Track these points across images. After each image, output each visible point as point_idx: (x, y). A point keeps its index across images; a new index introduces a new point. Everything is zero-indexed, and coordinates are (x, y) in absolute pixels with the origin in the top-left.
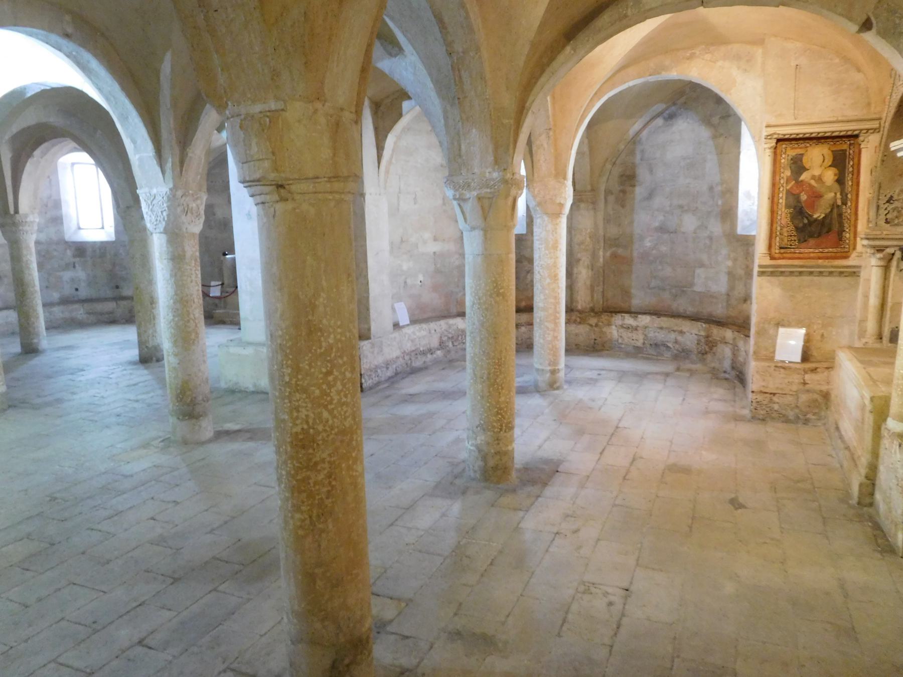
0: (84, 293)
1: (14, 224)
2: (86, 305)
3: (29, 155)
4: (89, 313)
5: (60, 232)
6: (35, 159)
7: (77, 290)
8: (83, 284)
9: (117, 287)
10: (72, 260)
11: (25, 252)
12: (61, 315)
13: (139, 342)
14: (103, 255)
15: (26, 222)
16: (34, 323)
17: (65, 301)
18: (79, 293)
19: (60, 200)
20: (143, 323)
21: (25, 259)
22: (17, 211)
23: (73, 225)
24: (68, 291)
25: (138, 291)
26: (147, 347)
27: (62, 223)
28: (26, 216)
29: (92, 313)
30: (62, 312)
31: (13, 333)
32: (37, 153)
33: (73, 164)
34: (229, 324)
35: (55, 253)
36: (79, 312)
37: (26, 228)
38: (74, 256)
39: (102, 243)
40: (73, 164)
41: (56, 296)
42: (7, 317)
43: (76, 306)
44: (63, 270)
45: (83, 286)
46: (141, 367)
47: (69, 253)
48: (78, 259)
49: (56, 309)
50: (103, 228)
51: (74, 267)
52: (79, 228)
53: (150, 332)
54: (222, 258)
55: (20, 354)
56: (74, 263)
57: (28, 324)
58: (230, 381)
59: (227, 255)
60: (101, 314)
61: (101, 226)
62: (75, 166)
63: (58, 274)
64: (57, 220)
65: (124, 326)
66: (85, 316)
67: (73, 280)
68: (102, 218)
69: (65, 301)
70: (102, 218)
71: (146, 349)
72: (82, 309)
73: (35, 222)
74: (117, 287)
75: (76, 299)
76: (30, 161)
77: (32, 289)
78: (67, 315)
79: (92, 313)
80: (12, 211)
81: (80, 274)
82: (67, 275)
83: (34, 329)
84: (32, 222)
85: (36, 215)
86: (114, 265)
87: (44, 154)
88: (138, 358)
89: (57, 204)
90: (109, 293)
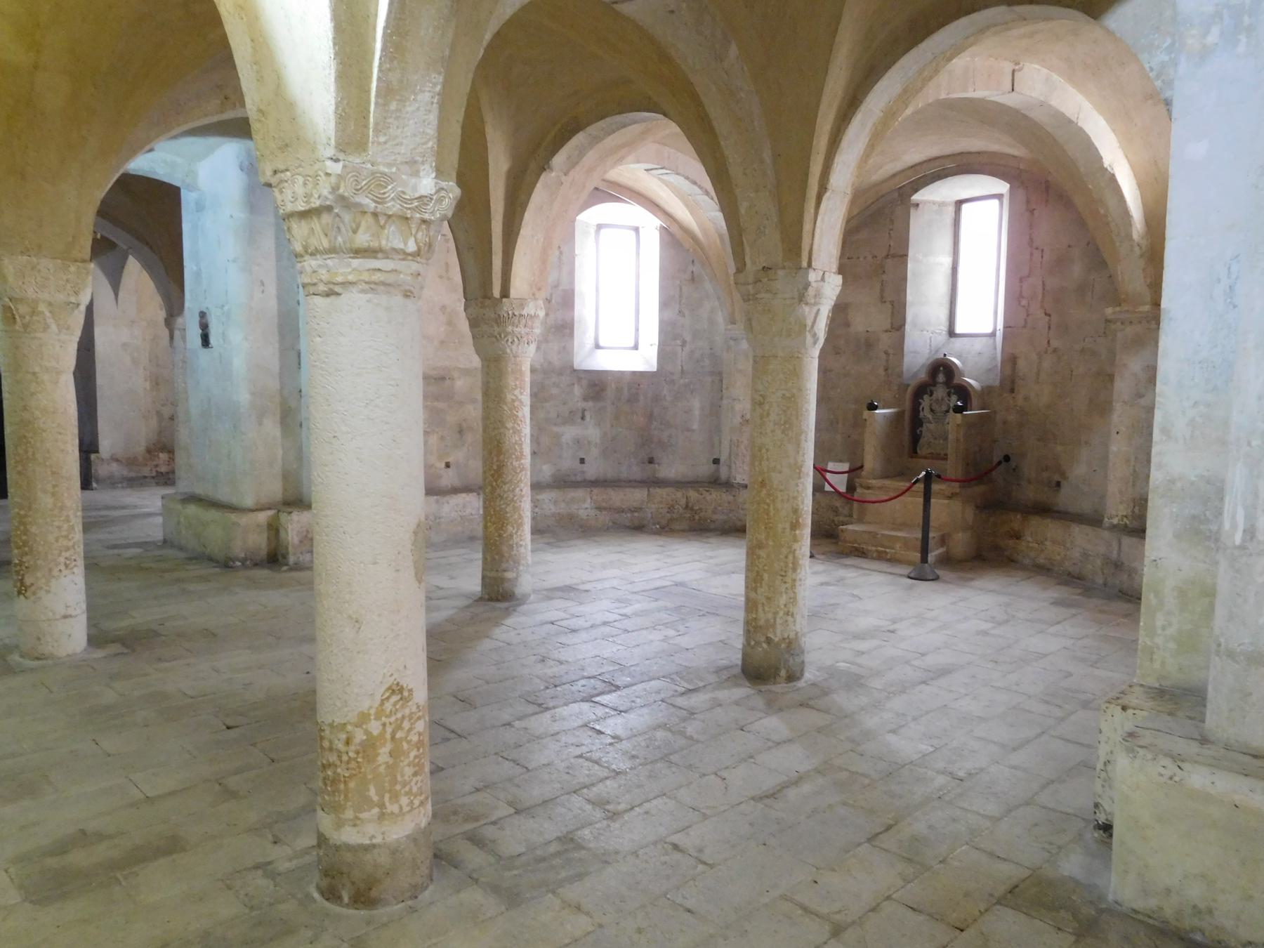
0: (593, 469)
1: (499, 320)
2: (596, 491)
3: (544, 167)
4: (599, 508)
5: (567, 351)
6: (553, 174)
7: (582, 461)
8: (595, 452)
9: (651, 461)
10: (582, 405)
11: (511, 381)
12: (553, 509)
13: (747, 623)
14: (633, 399)
15: (521, 315)
16: (511, 536)
17: (562, 482)
18: (585, 467)
19: (572, 291)
20: (766, 576)
21: (509, 397)
22: (505, 293)
23: (589, 341)
24: (568, 463)
25: (764, 492)
26: (769, 641)
27: (571, 334)
28: (522, 303)
29: (605, 509)
30: (555, 503)
31: (472, 539)
32: (559, 160)
33: (600, 227)
34: (873, 558)
35: (555, 391)
36: (583, 504)
37: (520, 330)
38: (585, 399)
39: (634, 373)
40: (600, 227)
41: (547, 471)
42: (464, 506)
43: (580, 493)
44: (564, 423)
45: (593, 454)
46: (743, 691)
47: (577, 391)
48: (590, 404)
49: (545, 496)
50: (636, 347)
51: (583, 418)
52: (597, 346)
53: (783, 600)
54: (866, 413)
55: (481, 599)
56: (584, 411)
57: (500, 536)
58: (1168, 891)
59: (876, 408)
60: (620, 511)
61: (632, 344)
62: (603, 231)
63: (556, 429)
64: (564, 329)
65: (661, 541)
66: (593, 512)
67: (578, 441)
68: (637, 330)
69: (562, 482)
70: (637, 330)
71: (765, 646)
72: (589, 500)
73: (536, 316)
74: (651, 461)
75: (579, 478)
76: (544, 178)
77: (516, 464)
78: (563, 508)
79: (605, 509)
80: (496, 292)
81: (592, 432)
82: (569, 433)
83: (511, 547)
84: (531, 317)
85: (541, 303)
86: (651, 417)
87: (573, 163)
88: (737, 658)
89: (568, 300)
90: (636, 472)
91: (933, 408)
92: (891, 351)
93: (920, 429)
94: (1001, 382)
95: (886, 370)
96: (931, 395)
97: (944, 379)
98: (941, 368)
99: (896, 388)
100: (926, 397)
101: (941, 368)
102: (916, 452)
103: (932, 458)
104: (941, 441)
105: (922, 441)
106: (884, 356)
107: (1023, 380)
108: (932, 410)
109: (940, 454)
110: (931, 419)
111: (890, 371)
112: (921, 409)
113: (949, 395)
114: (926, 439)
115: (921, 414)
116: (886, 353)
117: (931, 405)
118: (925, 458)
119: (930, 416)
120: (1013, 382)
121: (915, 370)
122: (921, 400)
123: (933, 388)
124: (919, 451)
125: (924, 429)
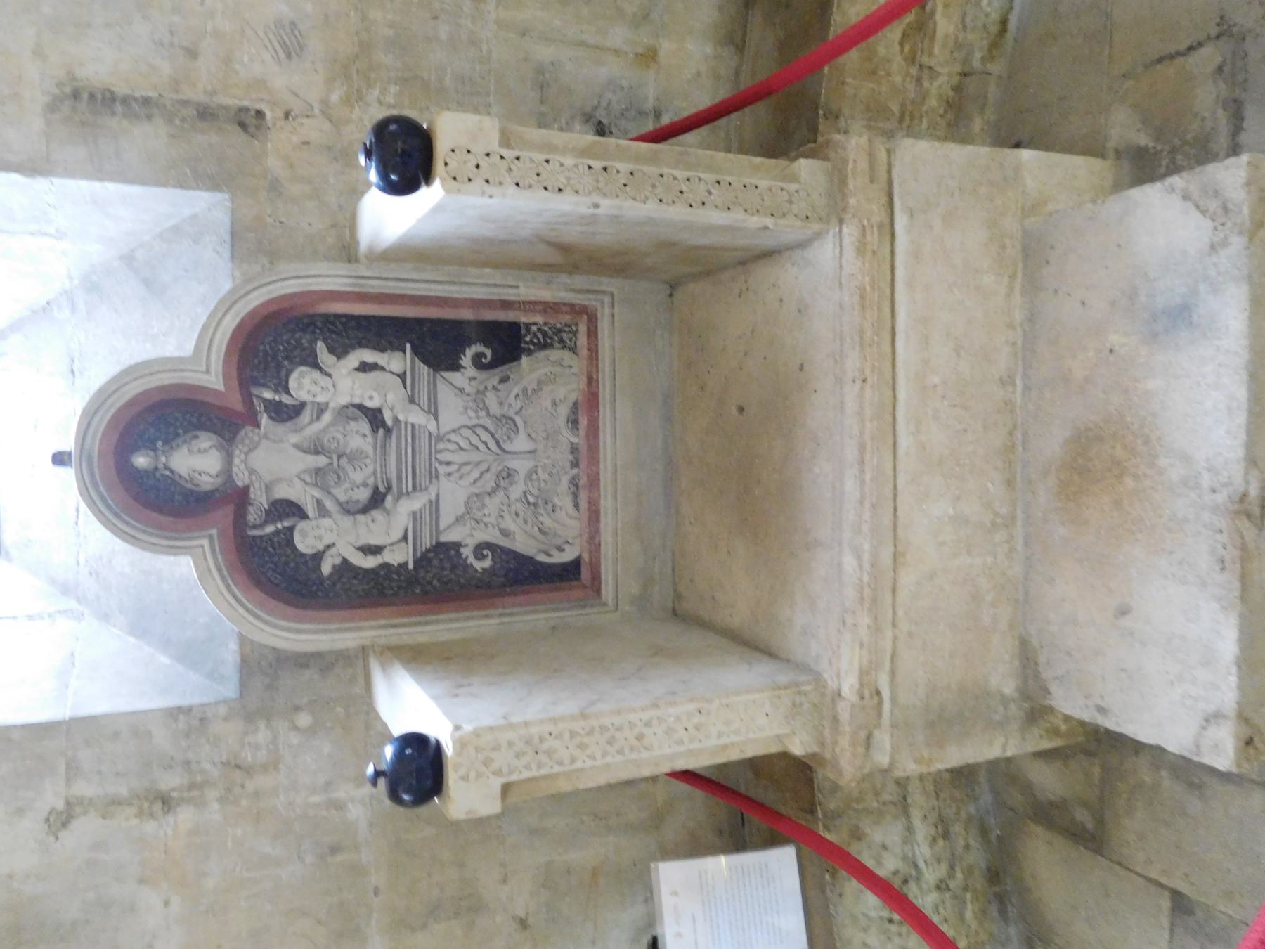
91: (363, 495)
92: (51, 797)
93: (467, 552)
94: (213, 183)
95: (166, 802)
96: (291, 509)
97: (206, 440)
98: (141, 461)
99: (262, 735)
100: (305, 542)
101: (141, 461)
102: (570, 572)
103: (594, 482)
104: (520, 443)
105: (524, 544)
106: (86, 827)
107: (192, 53)
108: (376, 500)
109: (574, 450)
110: (416, 503)
111: (170, 781)
112: (370, 562)
113: (286, 413)
114: (509, 523)
115: (395, 557)
116: (61, 820)
117: (349, 509)
118: (594, 516)
119: (402, 512)
120: (206, 114)
121: (164, 659)
122: (326, 569)
123: (260, 499)
124: (567, 556)
125: (466, 536)
